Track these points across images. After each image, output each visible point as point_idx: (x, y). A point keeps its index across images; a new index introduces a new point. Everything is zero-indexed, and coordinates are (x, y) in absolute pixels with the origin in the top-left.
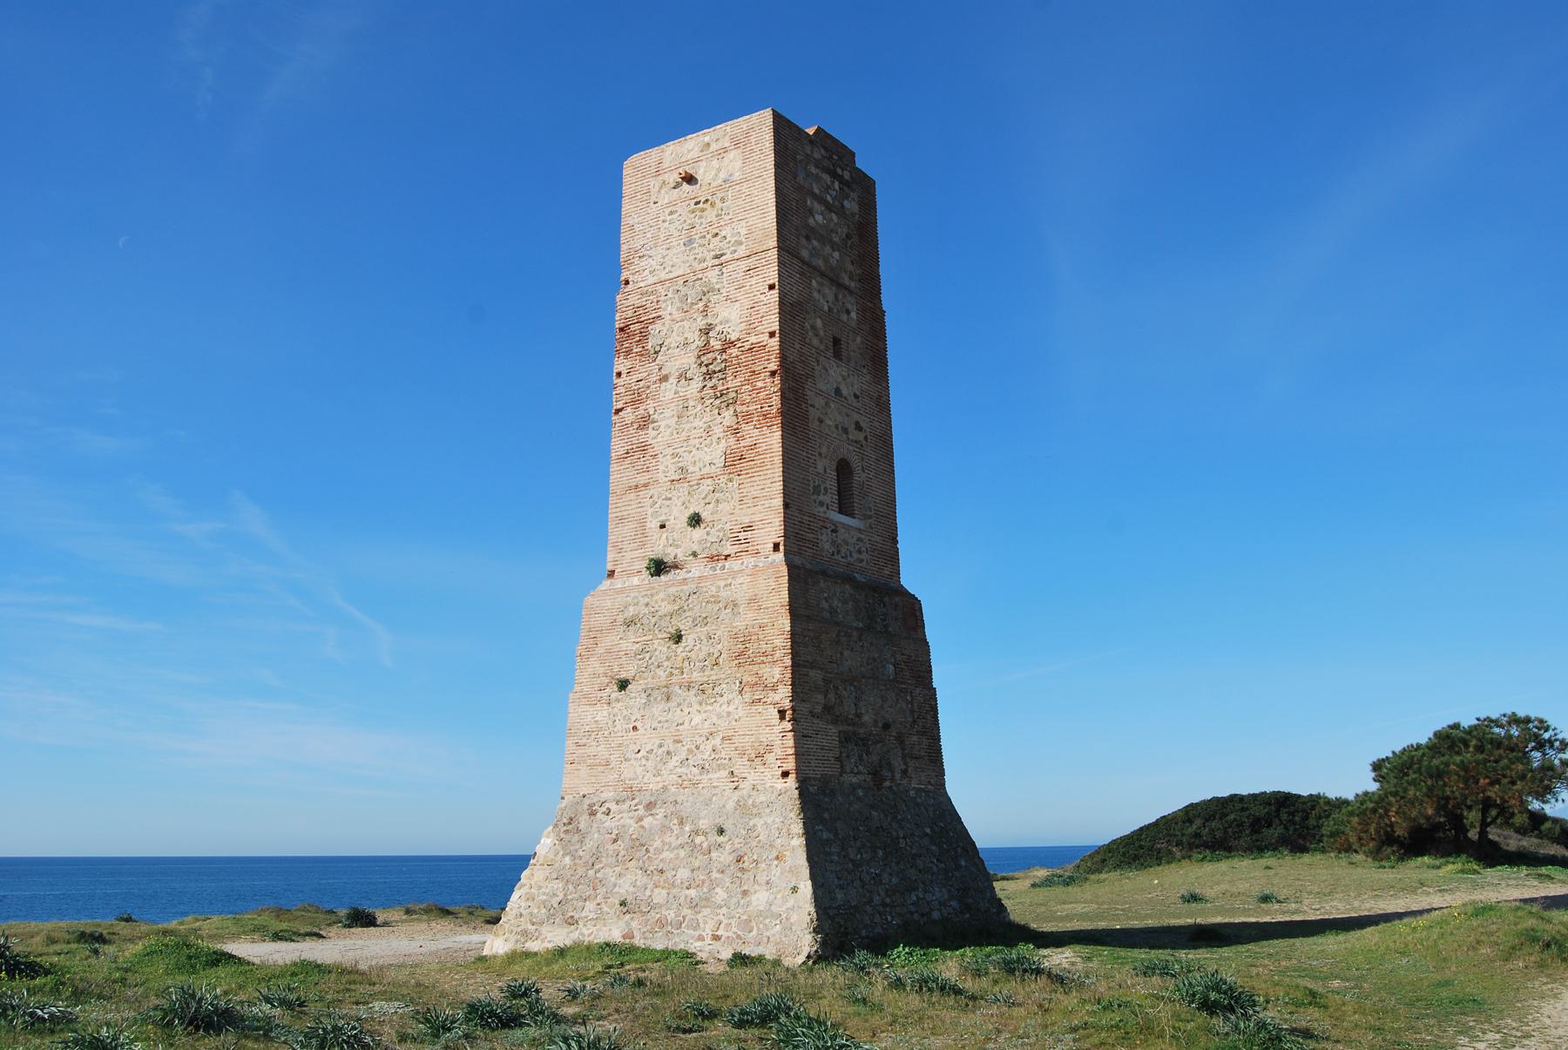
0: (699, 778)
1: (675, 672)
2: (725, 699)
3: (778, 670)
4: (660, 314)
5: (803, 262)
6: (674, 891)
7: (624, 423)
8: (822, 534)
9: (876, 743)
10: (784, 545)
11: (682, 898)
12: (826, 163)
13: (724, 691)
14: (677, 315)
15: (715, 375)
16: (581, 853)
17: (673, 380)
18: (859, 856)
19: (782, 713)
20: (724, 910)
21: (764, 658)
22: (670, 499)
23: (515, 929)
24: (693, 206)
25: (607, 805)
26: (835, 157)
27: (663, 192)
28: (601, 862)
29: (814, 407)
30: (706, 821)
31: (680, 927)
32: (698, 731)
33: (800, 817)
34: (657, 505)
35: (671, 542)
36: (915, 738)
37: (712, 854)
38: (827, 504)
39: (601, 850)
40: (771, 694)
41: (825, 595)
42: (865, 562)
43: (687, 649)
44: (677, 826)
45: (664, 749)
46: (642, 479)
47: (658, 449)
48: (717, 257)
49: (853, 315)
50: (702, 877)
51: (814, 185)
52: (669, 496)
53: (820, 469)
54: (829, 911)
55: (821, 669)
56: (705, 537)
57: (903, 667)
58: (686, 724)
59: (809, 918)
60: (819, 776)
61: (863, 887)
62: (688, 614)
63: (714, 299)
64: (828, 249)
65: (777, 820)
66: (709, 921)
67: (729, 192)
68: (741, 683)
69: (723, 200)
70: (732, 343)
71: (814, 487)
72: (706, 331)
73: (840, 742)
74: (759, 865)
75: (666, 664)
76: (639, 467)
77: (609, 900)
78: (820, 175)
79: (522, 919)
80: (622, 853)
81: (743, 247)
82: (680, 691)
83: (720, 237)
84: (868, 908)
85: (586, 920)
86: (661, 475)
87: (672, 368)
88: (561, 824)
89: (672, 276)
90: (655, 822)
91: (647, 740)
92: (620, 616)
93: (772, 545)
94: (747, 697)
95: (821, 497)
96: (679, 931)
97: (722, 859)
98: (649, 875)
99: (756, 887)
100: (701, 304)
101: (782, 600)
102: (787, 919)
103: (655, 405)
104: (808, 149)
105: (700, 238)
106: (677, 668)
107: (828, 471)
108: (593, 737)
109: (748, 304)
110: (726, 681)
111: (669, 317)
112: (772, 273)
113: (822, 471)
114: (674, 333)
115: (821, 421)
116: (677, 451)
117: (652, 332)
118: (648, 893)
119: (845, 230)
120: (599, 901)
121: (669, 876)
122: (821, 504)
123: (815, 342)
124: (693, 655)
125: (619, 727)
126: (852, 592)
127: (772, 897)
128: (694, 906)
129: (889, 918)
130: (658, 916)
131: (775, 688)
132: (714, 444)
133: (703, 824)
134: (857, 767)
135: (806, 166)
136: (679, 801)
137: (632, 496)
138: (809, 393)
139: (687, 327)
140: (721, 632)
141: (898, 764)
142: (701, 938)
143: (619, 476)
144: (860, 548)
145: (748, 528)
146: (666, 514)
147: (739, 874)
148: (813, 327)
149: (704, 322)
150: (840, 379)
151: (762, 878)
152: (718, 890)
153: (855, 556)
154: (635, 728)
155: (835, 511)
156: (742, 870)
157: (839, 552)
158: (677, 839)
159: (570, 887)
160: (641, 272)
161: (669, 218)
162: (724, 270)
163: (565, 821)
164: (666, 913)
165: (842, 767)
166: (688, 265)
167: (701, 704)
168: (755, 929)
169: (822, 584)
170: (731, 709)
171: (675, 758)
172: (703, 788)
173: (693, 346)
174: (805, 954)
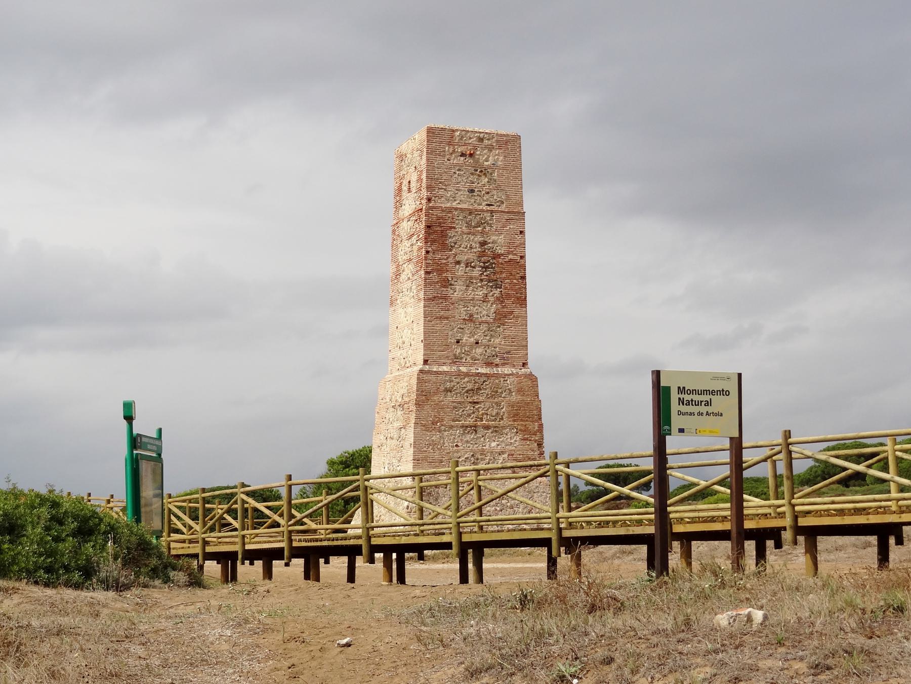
40: (534, 436)
72: (483, 244)
170: (512, 441)
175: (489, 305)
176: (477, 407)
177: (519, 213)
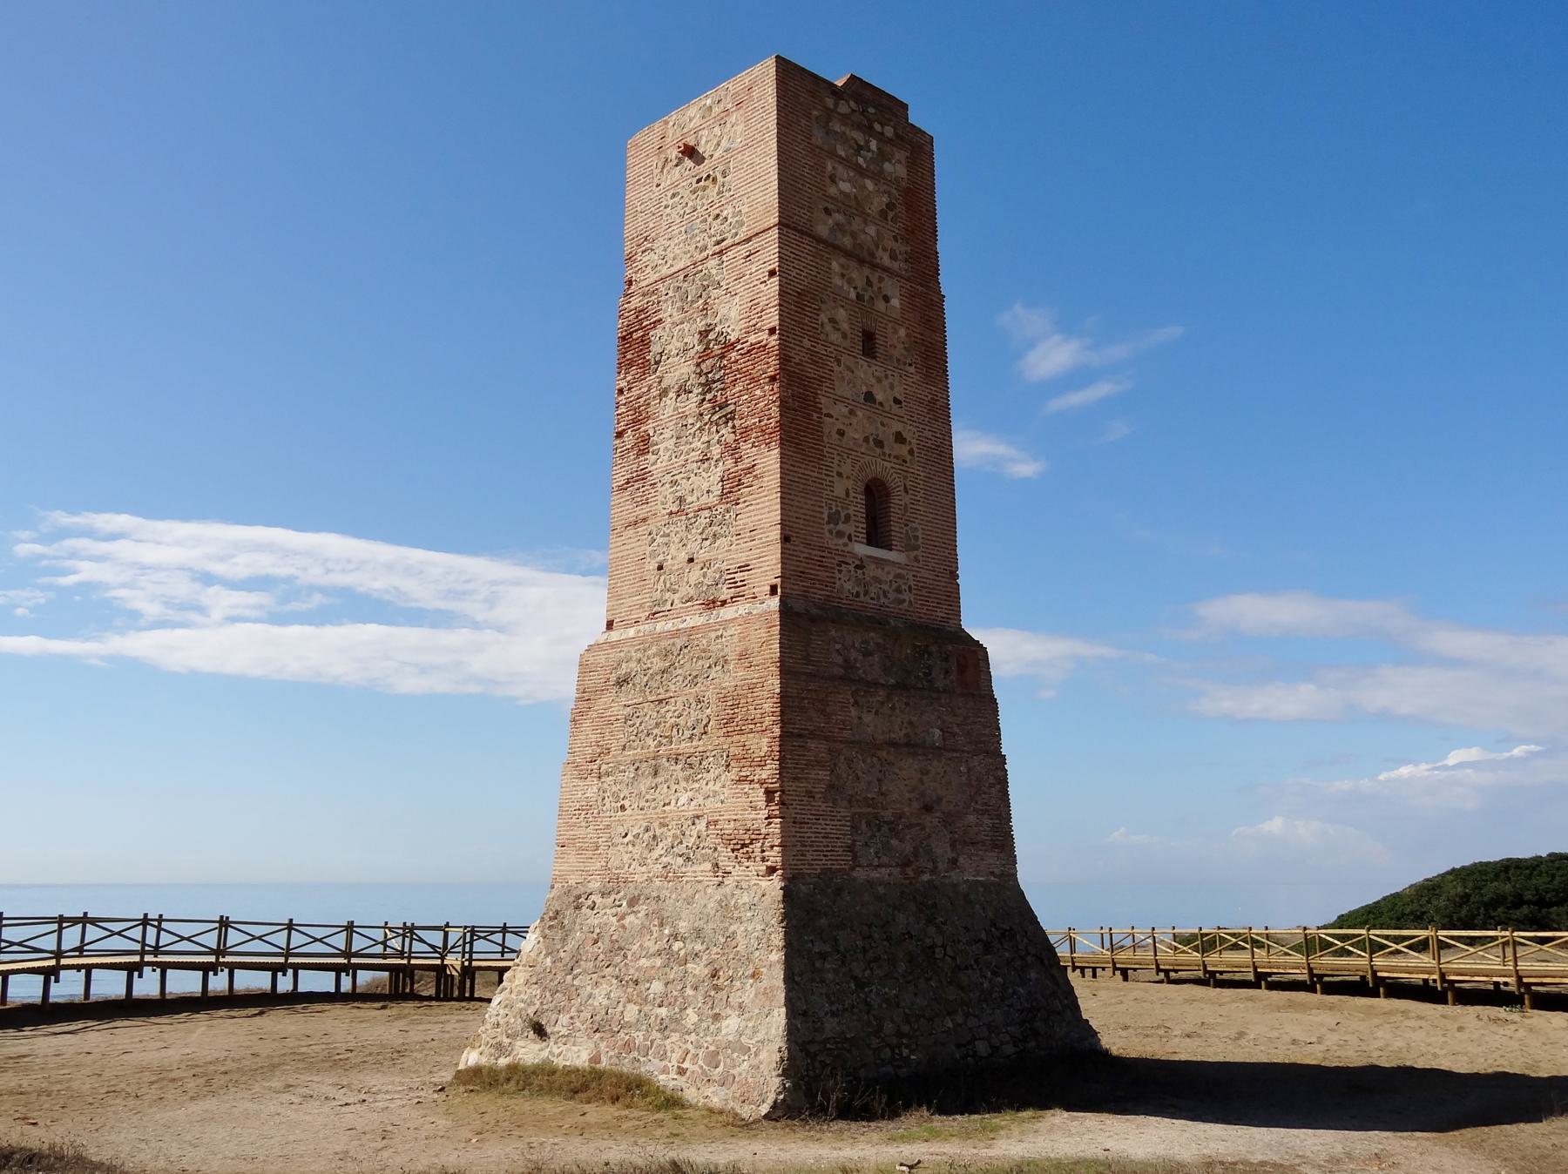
0: (684, 869)
1: (664, 741)
2: (711, 775)
3: (763, 743)
4: (661, 316)
5: (819, 240)
6: (646, 1009)
7: (625, 448)
8: (840, 571)
9: (910, 826)
10: (781, 588)
11: (653, 1018)
12: (857, 118)
13: (711, 764)
14: (677, 317)
15: (714, 386)
16: (562, 954)
17: (672, 394)
18: (867, 973)
19: (769, 793)
20: (693, 1037)
21: (753, 726)
22: (668, 535)
23: (491, 1042)
24: (695, 185)
25: (593, 897)
26: (871, 110)
27: (665, 171)
28: (579, 967)
29: (832, 417)
30: (684, 924)
31: (648, 1054)
32: (683, 813)
33: (782, 925)
34: (655, 544)
35: (668, 585)
36: (972, 818)
37: (688, 965)
38: (850, 535)
39: (581, 952)
41: (838, 646)
42: (906, 604)
43: (676, 714)
44: (657, 928)
45: (651, 833)
46: (642, 512)
47: (657, 475)
48: (718, 243)
49: (895, 302)
50: (675, 993)
51: (838, 146)
52: (667, 532)
53: (839, 490)
54: (808, 1047)
55: (826, 739)
56: (702, 579)
58: (673, 803)
59: (778, 1055)
60: (819, 871)
61: (868, 1013)
62: (679, 671)
63: (714, 293)
64: (857, 224)
65: (759, 927)
66: (677, 1049)
67: (731, 163)
68: (728, 756)
69: (724, 174)
70: (732, 344)
71: (830, 516)
72: (704, 334)
73: (852, 827)
74: (734, 982)
75: (656, 731)
76: (639, 499)
77: (582, 1014)
78: (848, 132)
79: (499, 1030)
80: (602, 957)
81: (744, 229)
82: (667, 764)
83: (721, 218)
84: (875, 1042)
85: (557, 1036)
86: (660, 507)
87: (670, 380)
88: (546, 917)
89: (673, 270)
90: (637, 921)
91: (634, 821)
92: (613, 675)
93: (769, 588)
94: (733, 775)
95: (841, 527)
96: (645, 1059)
97: (697, 972)
98: (623, 986)
99: (729, 1011)
100: (701, 301)
101: (773, 656)
102: (756, 1055)
103: (654, 424)
104: (830, 102)
105: (701, 222)
106: (667, 737)
107: (852, 494)
108: (583, 816)
109: (747, 296)
110: (713, 753)
111: (669, 320)
112: (772, 257)
113: (843, 495)
114: (675, 338)
115: (841, 433)
116: (675, 477)
117: (653, 338)
118: (620, 1008)
119: (885, 199)
120: (572, 1014)
121: (643, 989)
122: (840, 534)
123: (835, 337)
124: (681, 721)
125: (608, 805)
126: (880, 641)
127: (743, 1024)
128: (664, 1029)
129: (905, 1052)
130: (627, 1037)
131: (763, 763)
132: (712, 468)
133: (683, 926)
134: (879, 858)
135: (828, 123)
136: (662, 897)
137: (631, 532)
138: (823, 400)
139: (687, 330)
140: (710, 695)
141: (942, 849)
142: (665, 1071)
143: (620, 509)
144: (900, 586)
145: (744, 568)
146: (664, 553)
147: (713, 993)
148: (832, 320)
149: (703, 323)
150: (873, 381)
151: (734, 1000)
152: (689, 1011)
153: (892, 595)
154: (623, 808)
155: (862, 543)
156: (717, 988)
157: (866, 593)
158: (656, 943)
159: (548, 994)
160: (644, 269)
161: (671, 202)
162: (724, 258)
163: (551, 914)
164: (635, 1035)
165: (854, 858)
166: (689, 255)
167: (687, 780)
168: (722, 1064)
169: (833, 633)
170: (717, 788)
171: (661, 845)
172: (687, 882)
173: (692, 353)
174: (770, 1101)
175: (713, 462)
176: (663, 711)
177: (787, 226)
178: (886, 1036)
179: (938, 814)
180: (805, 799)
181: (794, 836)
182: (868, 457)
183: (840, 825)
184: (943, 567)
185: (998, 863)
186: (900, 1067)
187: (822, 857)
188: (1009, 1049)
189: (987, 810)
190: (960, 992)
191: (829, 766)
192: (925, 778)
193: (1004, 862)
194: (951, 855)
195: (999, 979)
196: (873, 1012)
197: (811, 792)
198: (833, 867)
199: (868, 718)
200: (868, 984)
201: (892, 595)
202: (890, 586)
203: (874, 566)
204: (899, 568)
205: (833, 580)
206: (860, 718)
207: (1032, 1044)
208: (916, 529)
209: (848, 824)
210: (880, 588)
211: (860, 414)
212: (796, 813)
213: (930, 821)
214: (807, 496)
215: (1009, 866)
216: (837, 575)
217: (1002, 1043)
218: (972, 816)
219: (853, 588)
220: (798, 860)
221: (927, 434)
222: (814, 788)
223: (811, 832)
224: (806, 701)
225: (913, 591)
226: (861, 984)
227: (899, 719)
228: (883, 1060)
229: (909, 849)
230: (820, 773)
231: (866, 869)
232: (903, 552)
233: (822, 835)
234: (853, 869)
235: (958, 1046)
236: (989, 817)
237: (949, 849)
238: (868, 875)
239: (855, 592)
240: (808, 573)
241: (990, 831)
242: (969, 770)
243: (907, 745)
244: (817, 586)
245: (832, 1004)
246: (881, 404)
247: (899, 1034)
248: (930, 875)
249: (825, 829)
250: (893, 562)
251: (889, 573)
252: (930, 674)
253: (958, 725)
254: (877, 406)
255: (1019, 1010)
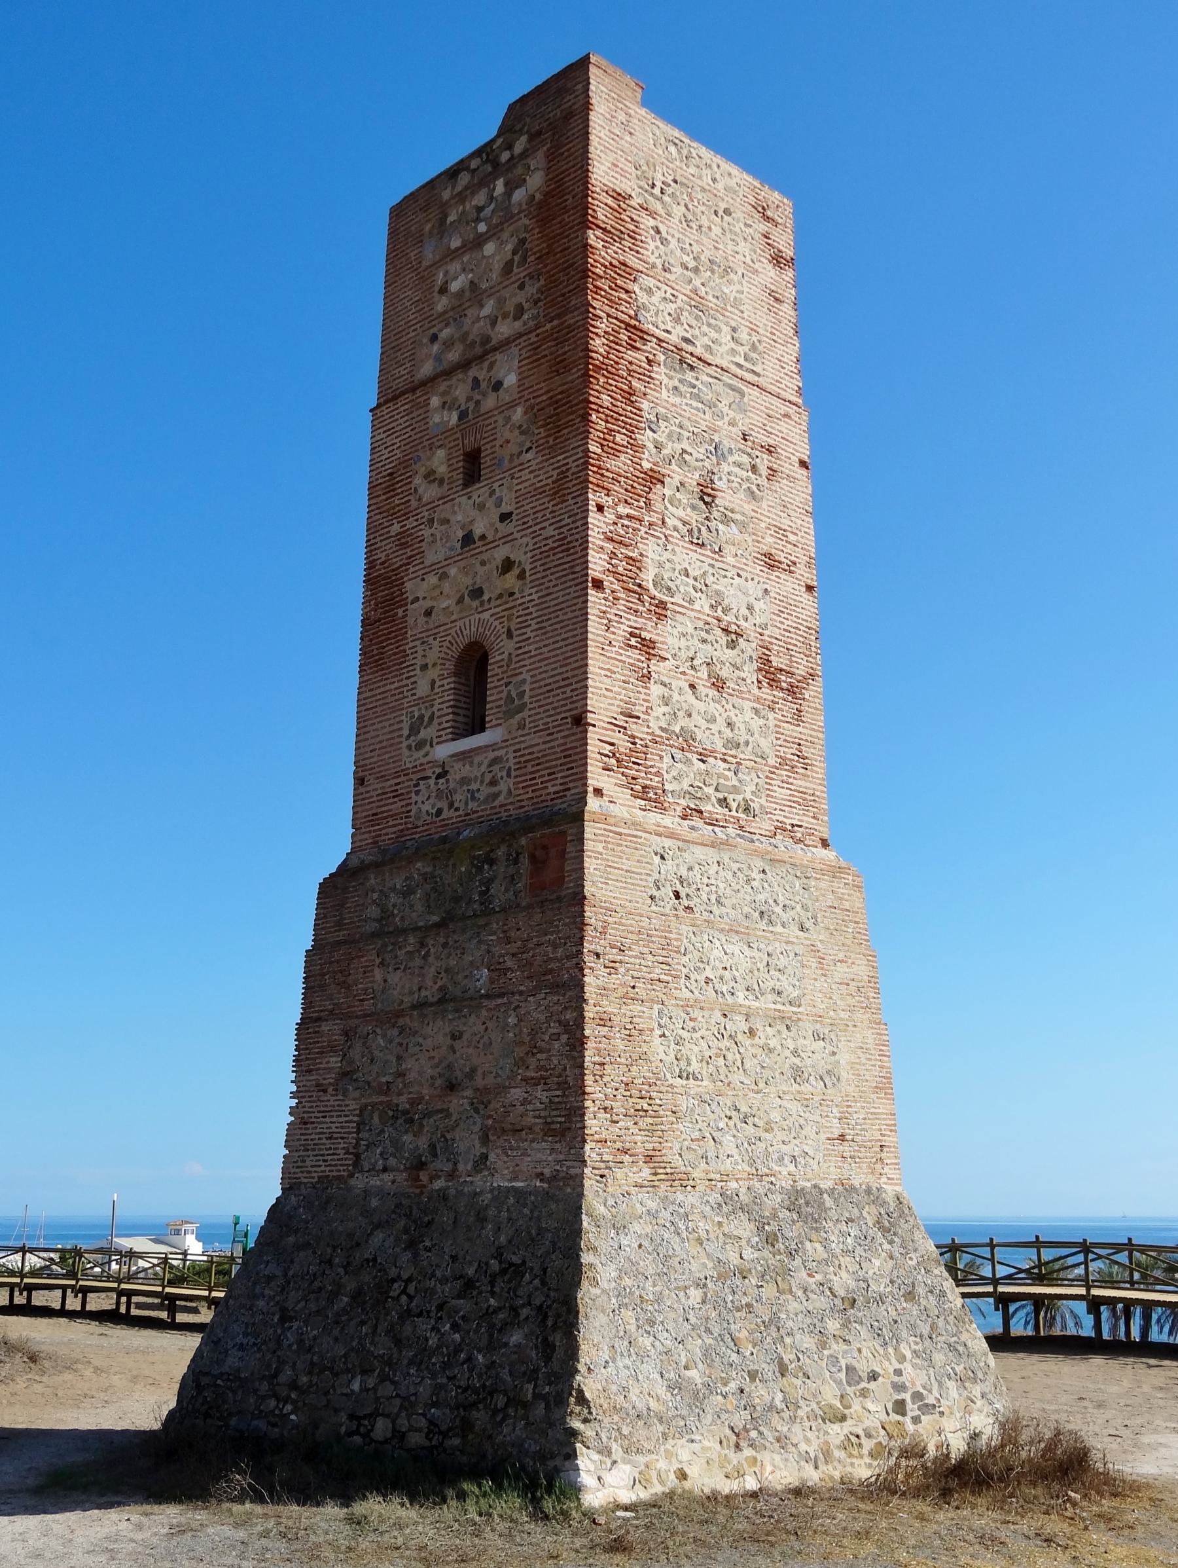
53: (423, 689)
57: (509, 964)
60: (316, 1180)
126: (429, 869)
141: (467, 1141)
157: (451, 805)
165: (357, 1163)
169: (373, 881)
178: (278, 1384)
179: (469, 1093)
180: (314, 1094)
181: (299, 1140)
182: (458, 624)
183: (346, 1122)
184: (559, 717)
185: (550, 1158)
186: (274, 1425)
187: (321, 1163)
188: (416, 1439)
189: (542, 1077)
190: (393, 1346)
191: (341, 1050)
192: (458, 1044)
193: (561, 1157)
194: (479, 1150)
195: (457, 1337)
196: (279, 1353)
197: (322, 1085)
198: (331, 1174)
199: (394, 978)
200: (291, 1319)
201: (485, 791)
202: (482, 782)
203: (461, 763)
204: (493, 750)
205: (409, 808)
206: (385, 981)
207: (456, 1441)
208: (524, 681)
209: (356, 1119)
210: (468, 790)
211: (453, 571)
212: (304, 1112)
213: (459, 1103)
214: (386, 717)
215: (568, 1163)
216: (414, 798)
217: (412, 1429)
218: (518, 1090)
219: (433, 807)
220: (298, 1167)
221: (550, 531)
222: (324, 1079)
223: (316, 1134)
224: (327, 977)
225: (513, 773)
226: (285, 1318)
227: (433, 969)
228: (261, 1411)
229: (423, 1142)
230: (332, 1059)
231: (366, 1174)
232: (500, 724)
233: (327, 1135)
234: (351, 1175)
235: (351, 1417)
236: (546, 1087)
237: (477, 1145)
238: (367, 1183)
239: (434, 811)
240: (380, 813)
241: (545, 1109)
242: (520, 1020)
243: (441, 1001)
244: (390, 824)
245: (245, 1335)
246: (483, 537)
247: (293, 1385)
248: (446, 1181)
249: (330, 1128)
250: (487, 746)
251: (480, 765)
252: (488, 890)
253: (513, 955)
254: (479, 543)
255: (460, 1387)
